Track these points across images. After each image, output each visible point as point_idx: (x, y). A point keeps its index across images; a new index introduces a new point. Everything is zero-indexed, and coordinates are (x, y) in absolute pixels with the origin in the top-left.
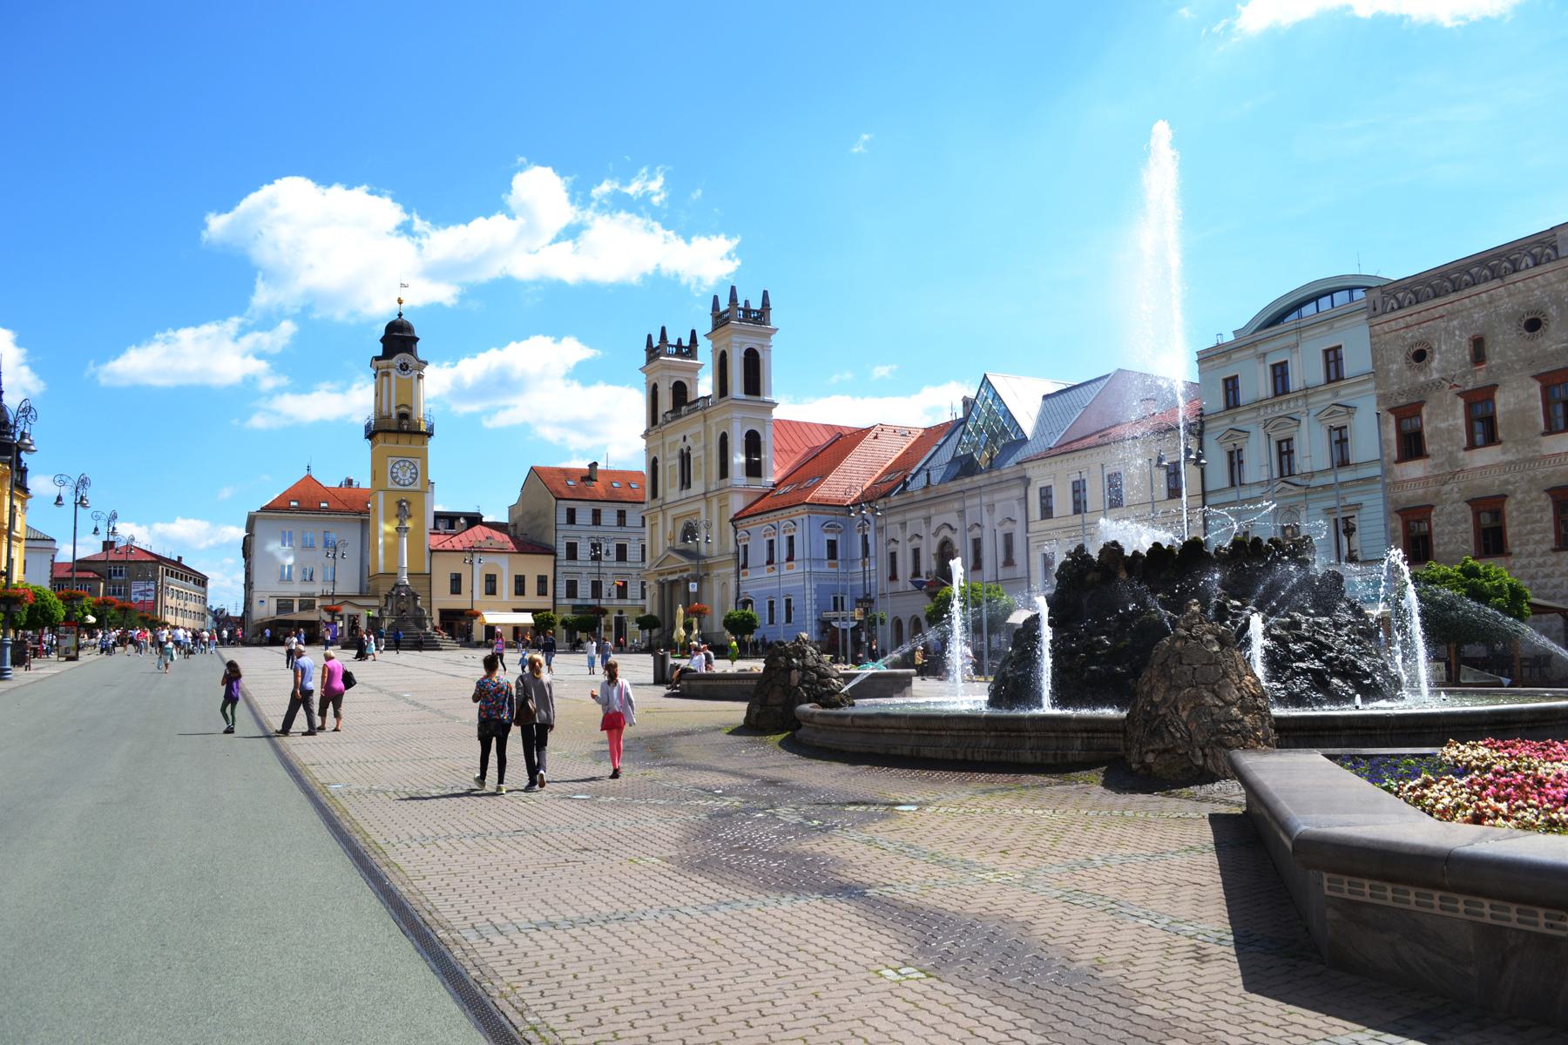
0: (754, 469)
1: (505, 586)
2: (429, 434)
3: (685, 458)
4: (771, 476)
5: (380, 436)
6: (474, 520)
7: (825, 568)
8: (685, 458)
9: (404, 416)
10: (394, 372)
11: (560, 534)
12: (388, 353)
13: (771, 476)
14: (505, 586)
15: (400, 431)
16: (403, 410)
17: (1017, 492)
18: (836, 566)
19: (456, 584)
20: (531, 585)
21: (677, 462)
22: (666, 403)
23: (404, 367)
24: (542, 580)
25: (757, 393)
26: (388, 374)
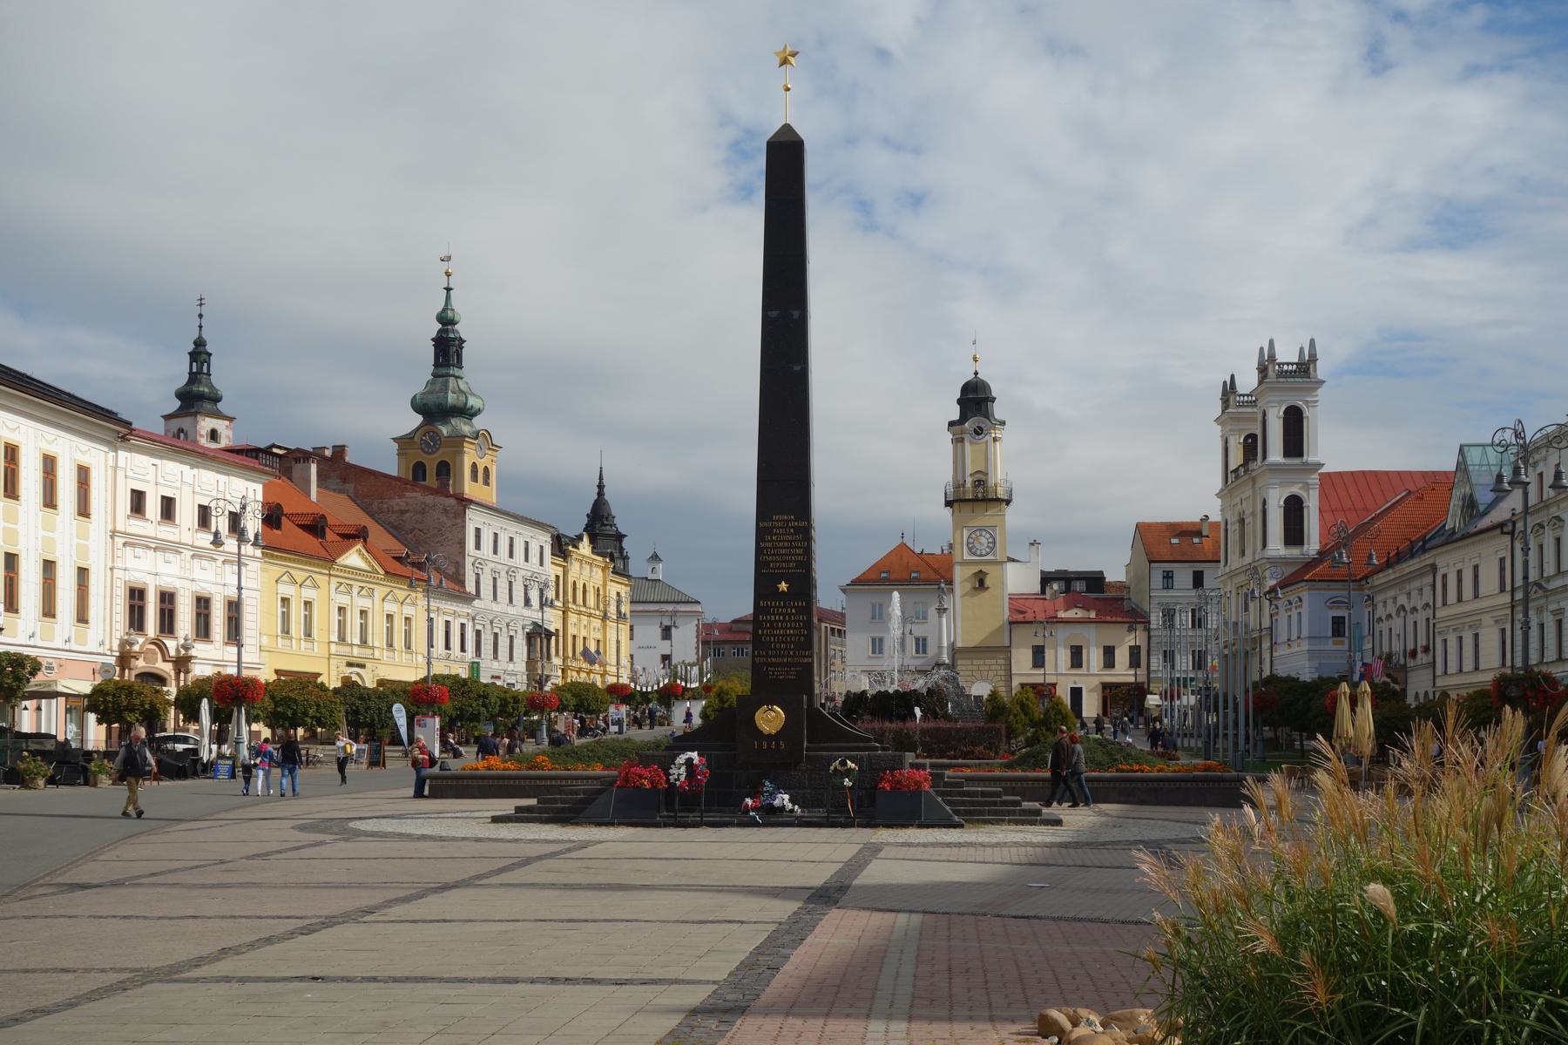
0: (1294, 535)
1: (1094, 657)
2: (1008, 502)
3: (1242, 521)
4: (1313, 545)
5: (956, 505)
6: (1095, 581)
7: (1330, 645)
8: (1242, 521)
9: (980, 483)
10: (967, 438)
11: (1154, 601)
12: (964, 418)
13: (1313, 545)
14: (1094, 657)
15: (976, 500)
16: (979, 476)
17: (1430, 579)
18: (1342, 643)
19: (1039, 658)
20: (1122, 656)
21: (1237, 526)
22: (1236, 459)
23: (979, 431)
24: (1135, 652)
25: (1300, 454)
26: (962, 440)
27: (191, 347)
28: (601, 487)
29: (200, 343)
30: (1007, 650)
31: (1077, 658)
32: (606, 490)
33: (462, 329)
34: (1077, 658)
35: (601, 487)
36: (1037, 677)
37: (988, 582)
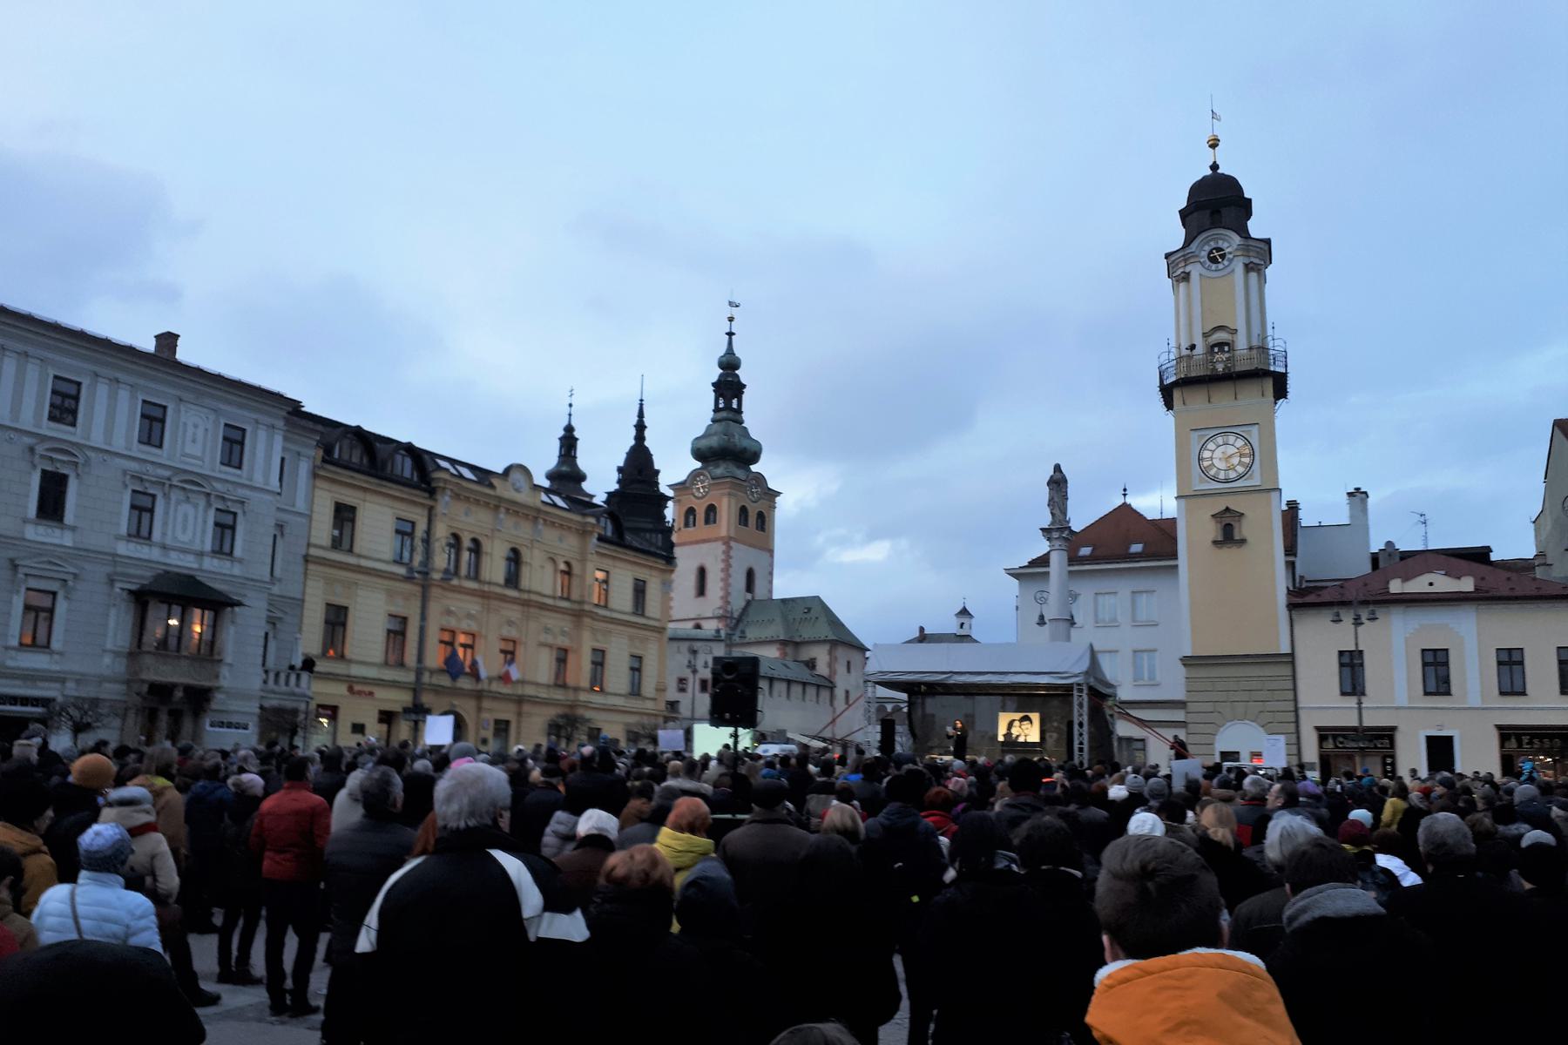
1: (1473, 674)
14: (1473, 674)
27: (561, 433)
28: (640, 427)
29: (569, 429)
30: (1290, 659)
31: (1436, 670)
32: (647, 433)
33: (743, 374)
34: (1436, 670)
35: (640, 427)
36: (1344, 714)
37: (1245, 530)
